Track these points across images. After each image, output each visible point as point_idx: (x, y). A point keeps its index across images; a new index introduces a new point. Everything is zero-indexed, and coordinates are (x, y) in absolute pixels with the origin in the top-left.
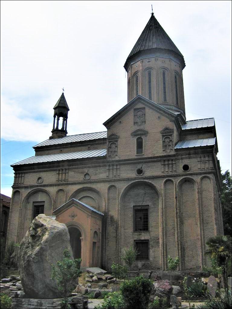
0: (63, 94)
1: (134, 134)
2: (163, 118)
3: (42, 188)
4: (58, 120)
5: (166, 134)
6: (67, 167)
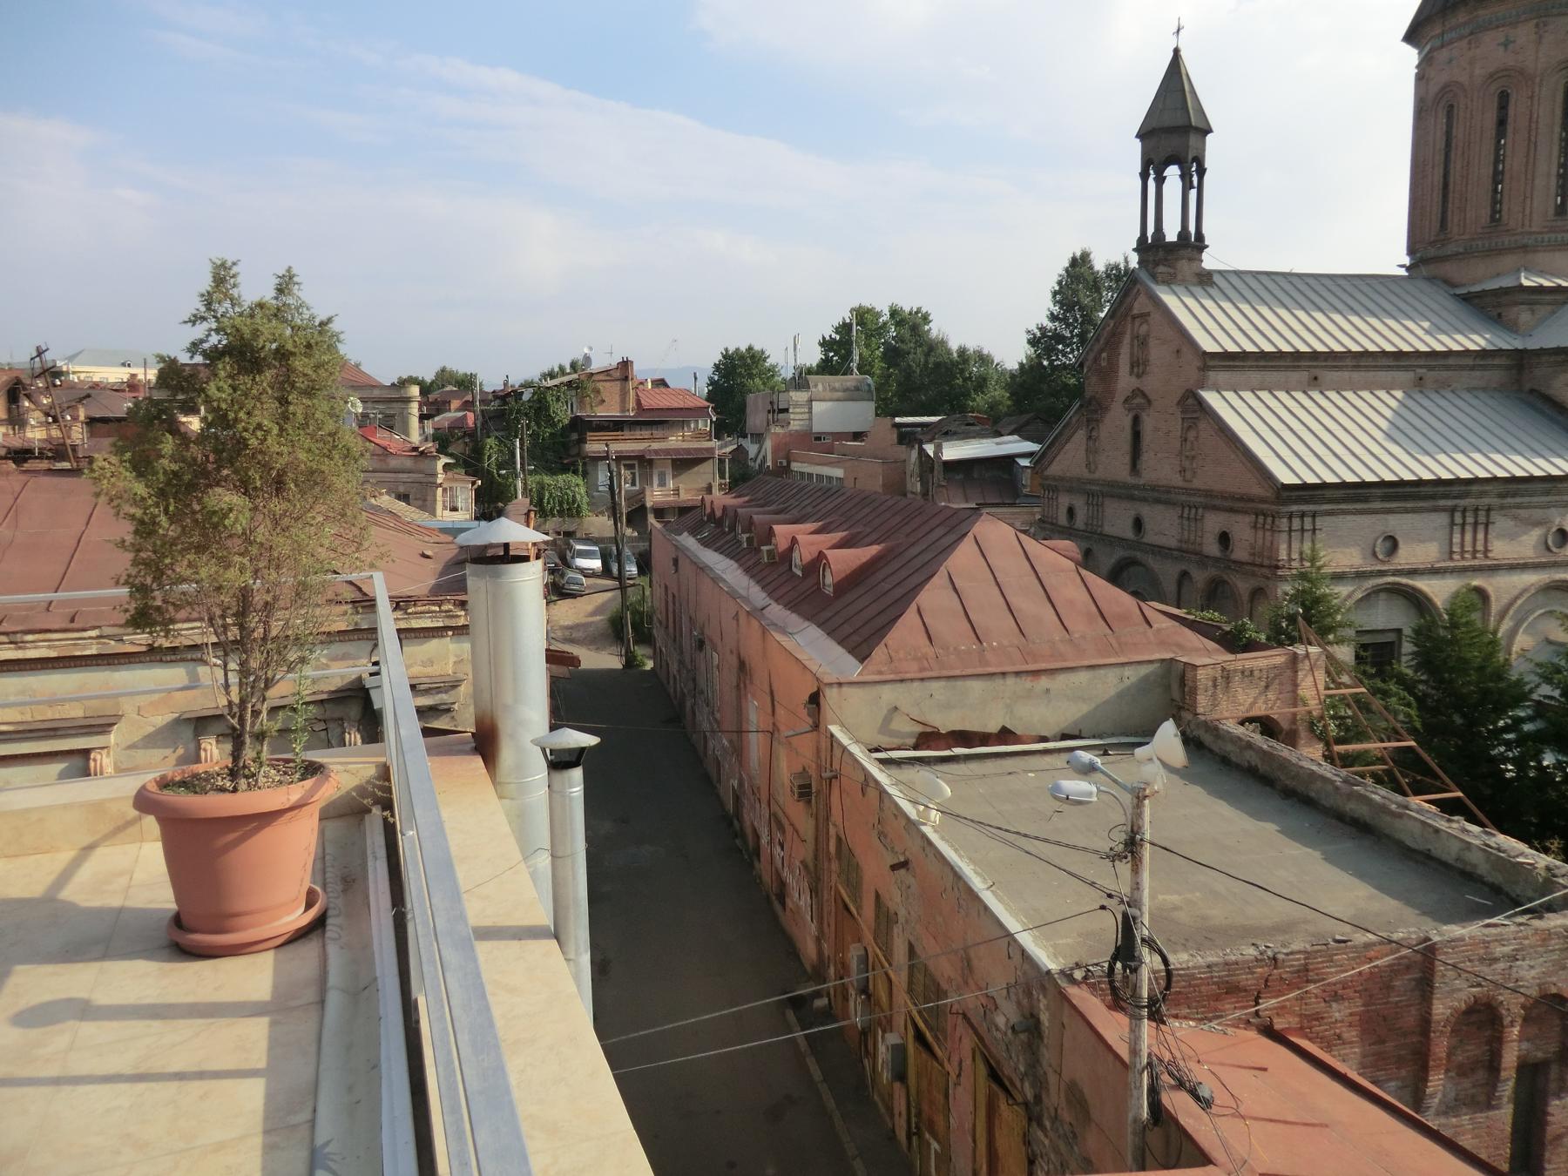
0: (1176, 51)
3: (1404, 580)
4: (1160, 180)
6: (1495, 501)
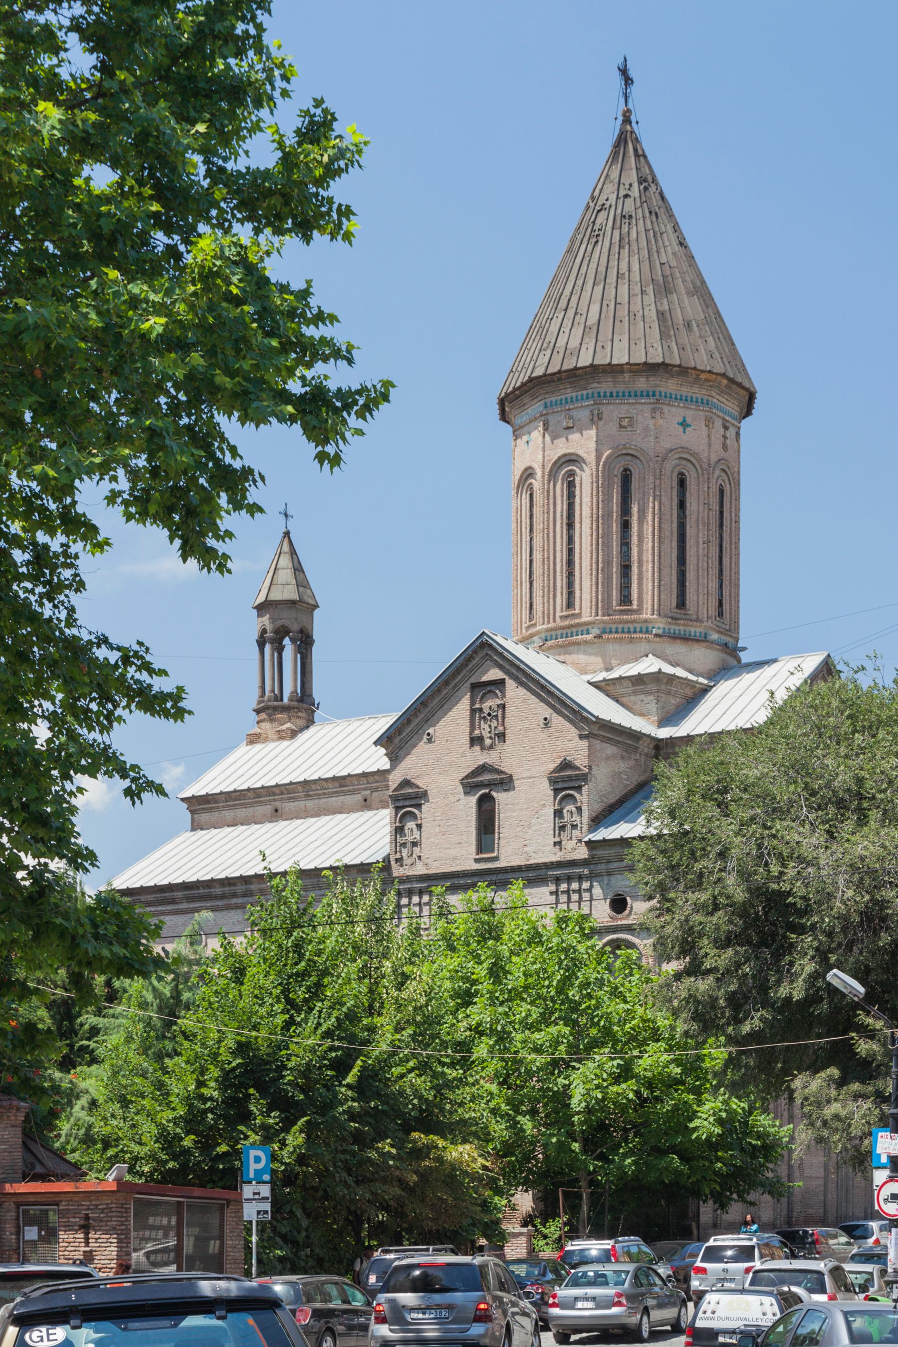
1: (470, 784)
2: (558, 721)
4: (280, 649)
5: (566, 785)
